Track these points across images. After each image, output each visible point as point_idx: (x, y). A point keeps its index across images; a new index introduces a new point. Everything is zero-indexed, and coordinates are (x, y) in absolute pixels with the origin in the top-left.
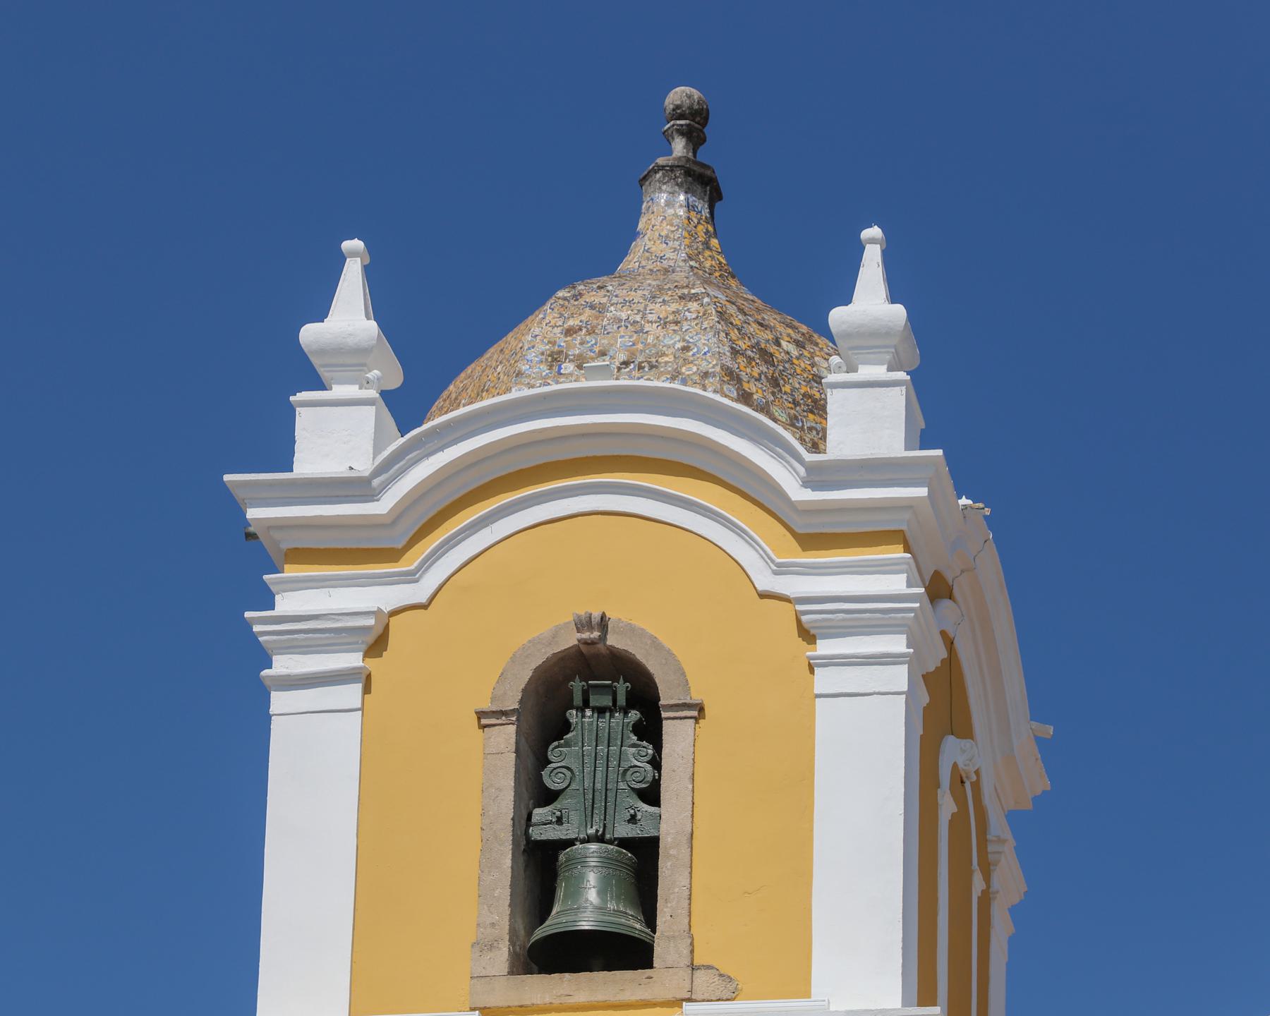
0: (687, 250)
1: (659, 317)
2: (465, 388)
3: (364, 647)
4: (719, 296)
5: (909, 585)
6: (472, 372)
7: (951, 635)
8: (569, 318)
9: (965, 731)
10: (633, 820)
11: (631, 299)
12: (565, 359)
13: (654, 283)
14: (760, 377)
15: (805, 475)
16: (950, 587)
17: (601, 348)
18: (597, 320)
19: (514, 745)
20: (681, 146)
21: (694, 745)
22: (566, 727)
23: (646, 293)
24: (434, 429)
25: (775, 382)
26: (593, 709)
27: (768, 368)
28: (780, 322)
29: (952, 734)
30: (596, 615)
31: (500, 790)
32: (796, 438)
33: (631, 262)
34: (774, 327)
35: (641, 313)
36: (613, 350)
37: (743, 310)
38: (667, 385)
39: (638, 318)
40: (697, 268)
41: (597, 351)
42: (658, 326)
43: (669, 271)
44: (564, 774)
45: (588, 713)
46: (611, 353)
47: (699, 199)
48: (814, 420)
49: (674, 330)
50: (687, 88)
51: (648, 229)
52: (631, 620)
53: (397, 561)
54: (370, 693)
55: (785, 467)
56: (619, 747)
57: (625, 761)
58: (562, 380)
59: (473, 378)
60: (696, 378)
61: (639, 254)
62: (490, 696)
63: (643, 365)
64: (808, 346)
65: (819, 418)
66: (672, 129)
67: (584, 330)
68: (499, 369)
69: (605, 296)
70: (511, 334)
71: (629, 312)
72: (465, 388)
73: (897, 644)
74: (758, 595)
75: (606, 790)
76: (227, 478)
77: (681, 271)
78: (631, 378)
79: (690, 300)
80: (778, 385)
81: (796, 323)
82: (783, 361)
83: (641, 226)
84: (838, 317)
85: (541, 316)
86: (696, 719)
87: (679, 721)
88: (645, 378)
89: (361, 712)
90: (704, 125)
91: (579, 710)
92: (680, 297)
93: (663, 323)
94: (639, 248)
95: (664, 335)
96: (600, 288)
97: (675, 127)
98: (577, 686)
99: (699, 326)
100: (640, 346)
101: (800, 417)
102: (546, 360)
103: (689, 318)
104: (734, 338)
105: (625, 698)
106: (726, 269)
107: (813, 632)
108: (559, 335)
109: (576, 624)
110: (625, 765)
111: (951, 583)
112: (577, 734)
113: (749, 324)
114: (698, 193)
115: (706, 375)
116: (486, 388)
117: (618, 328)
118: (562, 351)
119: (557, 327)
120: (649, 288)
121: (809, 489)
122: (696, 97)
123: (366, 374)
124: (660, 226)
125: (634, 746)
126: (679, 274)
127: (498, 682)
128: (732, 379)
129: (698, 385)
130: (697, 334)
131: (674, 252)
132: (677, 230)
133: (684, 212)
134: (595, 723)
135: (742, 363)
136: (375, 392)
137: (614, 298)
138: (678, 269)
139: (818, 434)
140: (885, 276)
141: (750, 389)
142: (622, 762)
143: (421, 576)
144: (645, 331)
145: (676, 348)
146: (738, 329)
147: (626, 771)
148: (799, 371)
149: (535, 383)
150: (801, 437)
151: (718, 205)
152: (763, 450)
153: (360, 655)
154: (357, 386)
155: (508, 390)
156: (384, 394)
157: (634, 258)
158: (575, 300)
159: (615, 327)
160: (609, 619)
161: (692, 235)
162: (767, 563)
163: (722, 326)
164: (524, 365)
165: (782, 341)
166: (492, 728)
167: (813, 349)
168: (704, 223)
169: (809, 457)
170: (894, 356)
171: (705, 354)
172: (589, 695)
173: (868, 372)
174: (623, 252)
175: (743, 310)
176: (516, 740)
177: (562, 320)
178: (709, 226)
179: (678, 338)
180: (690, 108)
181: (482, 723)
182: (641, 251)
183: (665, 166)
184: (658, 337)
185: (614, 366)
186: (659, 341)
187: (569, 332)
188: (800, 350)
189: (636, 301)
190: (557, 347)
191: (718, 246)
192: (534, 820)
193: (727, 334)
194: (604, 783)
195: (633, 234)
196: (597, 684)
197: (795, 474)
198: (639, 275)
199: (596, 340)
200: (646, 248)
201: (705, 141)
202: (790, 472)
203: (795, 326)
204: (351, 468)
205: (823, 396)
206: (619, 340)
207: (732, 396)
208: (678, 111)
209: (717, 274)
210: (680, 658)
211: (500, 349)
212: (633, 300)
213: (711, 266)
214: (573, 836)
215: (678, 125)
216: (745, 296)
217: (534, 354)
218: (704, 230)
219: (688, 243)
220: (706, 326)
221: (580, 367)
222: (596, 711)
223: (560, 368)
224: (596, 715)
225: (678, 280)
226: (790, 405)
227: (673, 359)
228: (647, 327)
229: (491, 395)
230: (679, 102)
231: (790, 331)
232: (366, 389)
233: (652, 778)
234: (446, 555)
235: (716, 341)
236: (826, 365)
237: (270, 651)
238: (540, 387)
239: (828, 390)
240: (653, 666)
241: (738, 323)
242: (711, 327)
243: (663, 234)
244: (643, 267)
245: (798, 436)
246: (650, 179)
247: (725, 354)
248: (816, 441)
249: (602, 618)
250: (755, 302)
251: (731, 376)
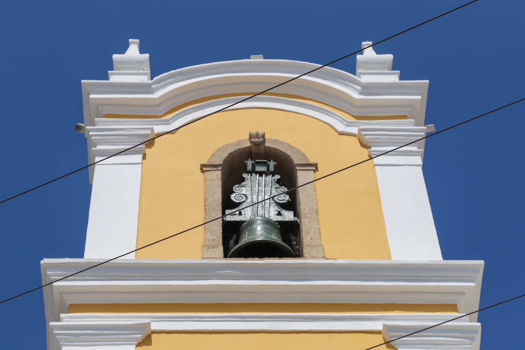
86: (315, 171)
87: (305, 171)
127: (211, 157)
162: (342, 122)
166: (208, 172)
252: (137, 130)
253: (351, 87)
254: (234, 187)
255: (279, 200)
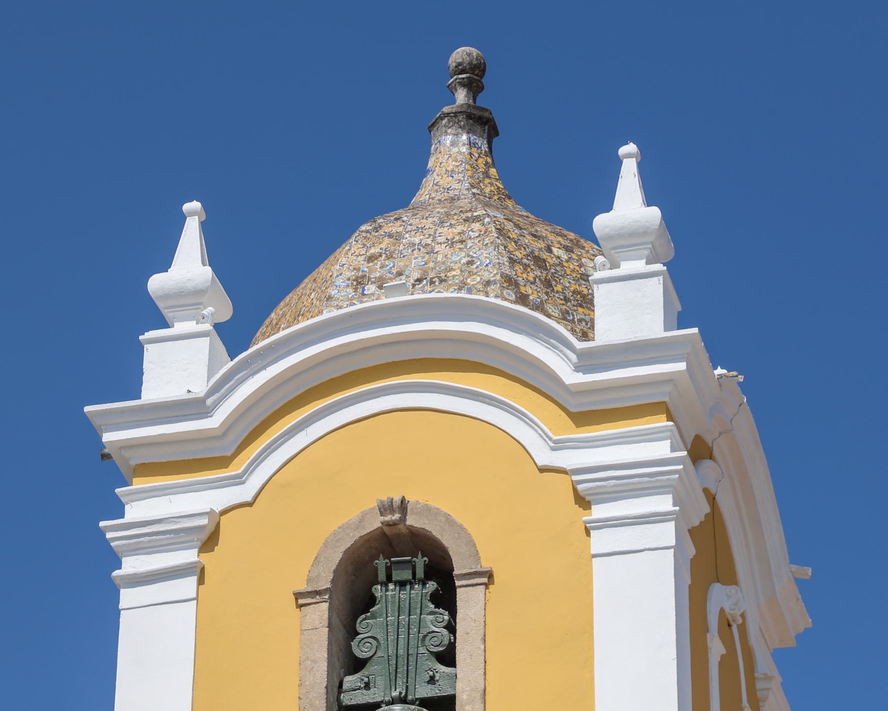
0: (470, 180)
1: (447, 239)
2: (284, 315)
3: (199, 544)
4: (498, 216)
5: (673, 449)
6: (290, 300)
7: (713, 491)
8: (371, 247)
9: (729, 577)
10: (432, 680)
11: (423, 226)
12: (368, 283)
13: (442, 210)
14: (535, 280)
15: (577, 361)
16: (709, 448)
17: (398, 270)
18: (395, 246)
19: (327, 620)
20: (463, 95)
21: (485, 609)
22: (372, 601)
23: (436, 219)
24: (258, 351)
25: (548, 284)
26: (396, 583)
27: (541, 272)
28: (551, 232)
29: (718, 582)
30: (397, 499)
31: (314, 661)
32: (568, 330)
33: (423, 195)
34: (546, 237)
35: (432, 237)
36: (409, 270)
37: (518, 225)
38: (455, 295)
39: (429, 241)
40: (479, 194)
41: (395, 273)
42: (446, 247)
43: (455, 199)
44: (370, 643)
45: (391, 586)
46: (407, 273)
47: (479, 137)
48: (583, 313)
49: (459, 248)
50: (467, 48)
51: (436, 166)
52: (427, 501)
53: (227, 467)
54: (203, 584)
55: (559, 355)
56: (419, 615)
57: (424, 628)
58: (365, 299)
59: (290, 306)
60: (480, 287)
61: (429, 188)
62: (306, 578)
63: (434, 280)
64: (577, 251)
65: (587, 311)
66: (455, 82)
67: (384, 256)
68: (312, 296)
69: (401, 226)
70: (322, 266)
71: (421, 237)
72: (284, 315)
73: (664, 503)
74: (539, 469)
75: (408, 655)
76: (87, 409)
77: (465, 198)
78: (424, 292)
79: (473, 222)
80: (551, 286)
81: (565, 232)
82: (555, 265)
83: (430, 164)
84: (601, 223)
85: (347, 248)
86: (486, 585)
88: (435, 291)
89: (195, 601)
90: (482, 76)
91: (383, 585)
92: (465, 220)
93: (451, 243)
94: (430, 182)
95: (452, 253)
96: (396, 219)
97: (458, 80)
98: (381, 563)
99: (481, 242)
100: (431, 265)
101: (570, 312)
102: (352, 284)
103: (472, 237)
104: (512, 249)
105: (423, 571)
106: (503, 193)
107: (588, 498)
108: (362, 262)
109: (379, 509)
110: (424, 631)
111: (710, 445)
112: (382, 607)
113: (524, 236)
114: (478, 132)
115: (488, 283)
116: (301, 313)
117: (412, 251)
118: (366, 276)
119: (361, 255)
120: (438, 215)
121: (581, 373)
122: (474, 54)
123: (202, 311)
124: (447, 163)
125: (432, 613)
126: (463, 200)
127: (312, 566)
128: (510, 285)
129: (481, 293)
130: (479, 250)
131: (459, 183)
132: (461, 164)
133: (466, 149)
134: (397, 596)
135: (519, 270)
136: (209, 325)
137: (408, 226)
138: (462, 197)
139: (587, 324)
140: (641, 184)
141: (526, 291)
142: (421, 629)
143: (247, 479)
144: (435, 252)
145: (462, 263)
146: (515, 242)
147: (425, 637)
148: (568, 272)
149: (342, 305)
150: (572, 328)
151: (495, 140)
152: (539, 342)
153: (196, 551)
154: (194, 322)
155: (320, 312)
156: (217, 326)
157: (425, 191)
158: (376, 232)
159: (410, 251)
160: (409, 501)
161: (474, 168)
163: (501, 240)
164: (333, 290)
165: (553, 248)
167: (581, 252)
168: (484, 157)
169: (579, 345)
170: (651, 251)
171: (487, 265)
172: (392, 573)
173: (628, 267)
174: (416, 187)
175: (518, 225)
176: (329, 615)
177: (365, 249)
178: (488, 158)
179: (463, 254)
180: (470, 64)
181: (299, 603)
182: (431, 185)
183: (450, 114)
184: (446, 255)
185: (409, 283)
186: (448, 258)
187: (371, 259)
188: (569, 254)
189: (427, 227)
190: (360, 273)
191: (496, 174)
192: (345, 687)
193: (505, 247)
194: (406, 649)
195: (424, 172)
196: (399, 560)
197: (568, 362)
198: (429, 205)
199: (394, 263)
200: (435, 182)
201: (483, 88)
202: (563, 359)
203: (563, 234)
204: (189, 391)
205: (590, 291)
206: (414, 261)
207: (510, 299)
208: (460, 67)
209: (496, 197)
210: (470, 531)
211: (313, 279)
212: (425, 226)
213: (490, 191)
214: (379, 699)
215: (460, 79)
216: (520, 213)
217: (341, 280)
218: (484, 162)
219: (471, 175)
220: (487, 242)
221: (380, 287)
222: (398, 585)
223: (364, 290)
224: (398, 588)
225: (462, 205)
226: (562, 302)
227: (459, 272)
228: (437, 248)
229: (306, 318)
230: (460, 60)
231: (560, 239)
232: (202, 323)
233: (448, 641)
234: (268, 458)
235: (496, 254)
236: (592, 265)
237: (120, 555)
238: (347, 307)
239: (595, 286)
240: (447, 540)
241: (515, 236)
242: (492, 243)
243: (449, 169)
244: (433, 199)
245: (569, 328)
246: (438, 125)
247: (504, 264)
248: (586, 331)
249: (402, 502)
250: (529, 217)
251: (510, 282)
252: (185, 519)
253: (561, 351)
254: (358, 625)
255: (435, 637)
